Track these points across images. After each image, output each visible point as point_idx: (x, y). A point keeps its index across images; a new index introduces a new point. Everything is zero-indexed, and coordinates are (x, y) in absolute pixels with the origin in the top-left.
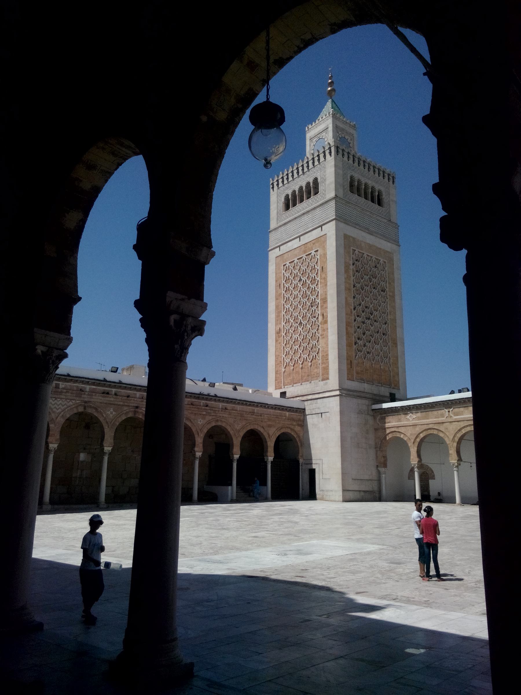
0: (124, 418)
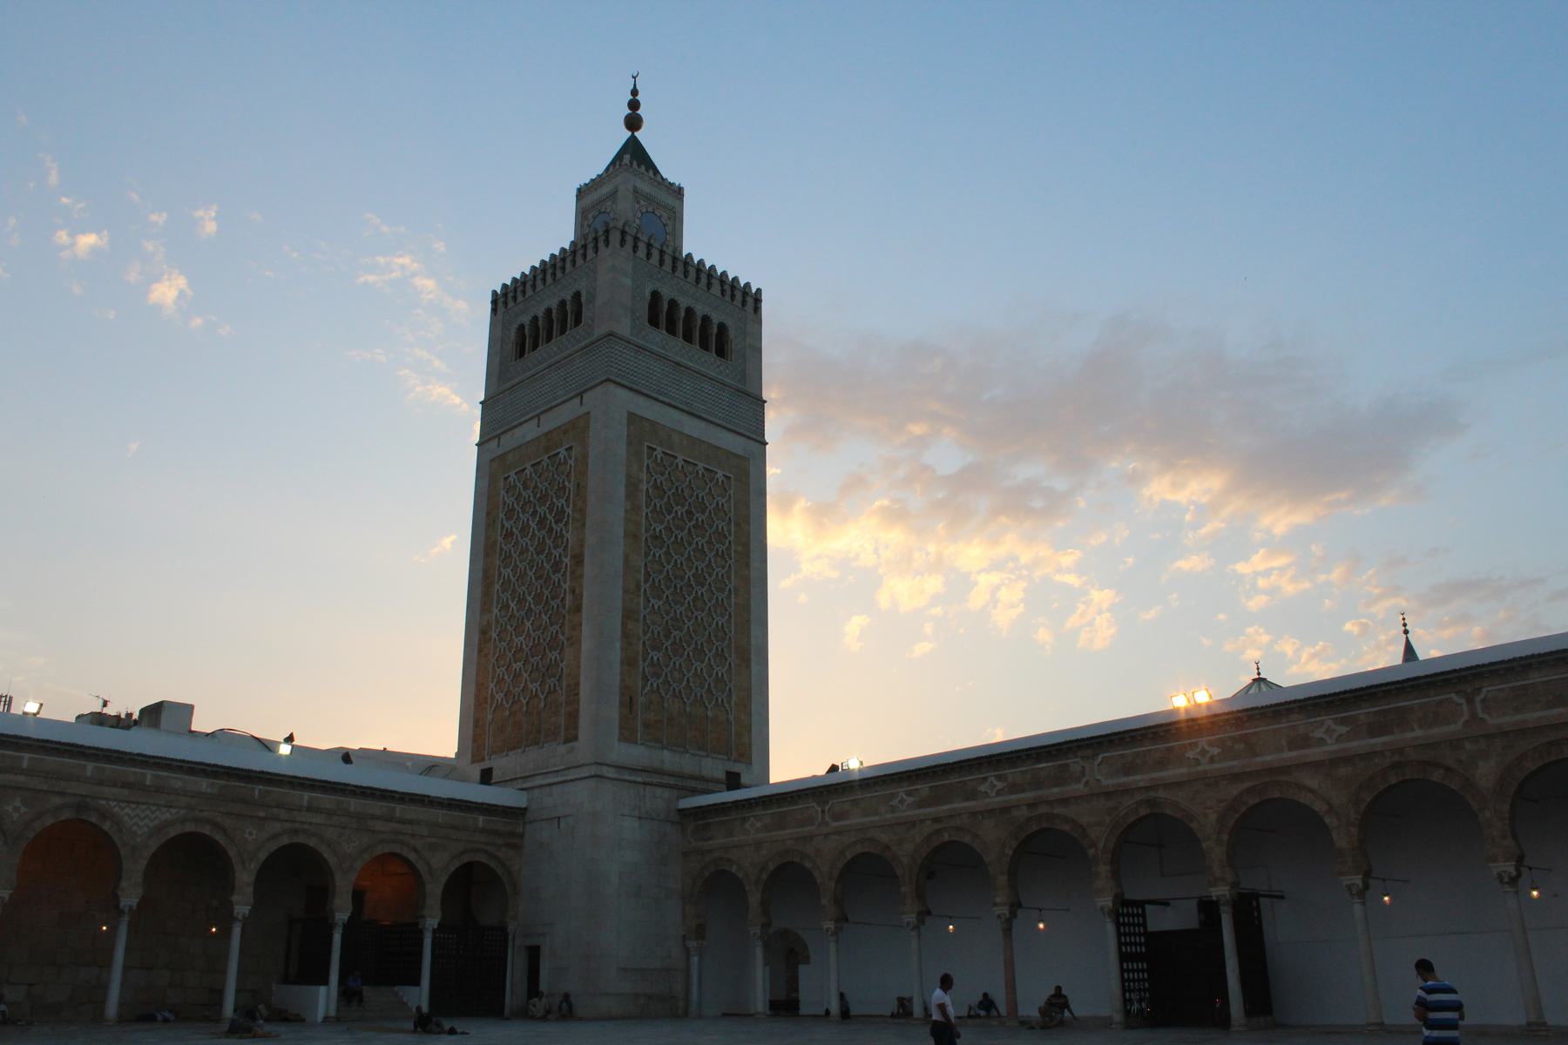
0: (49, 821)
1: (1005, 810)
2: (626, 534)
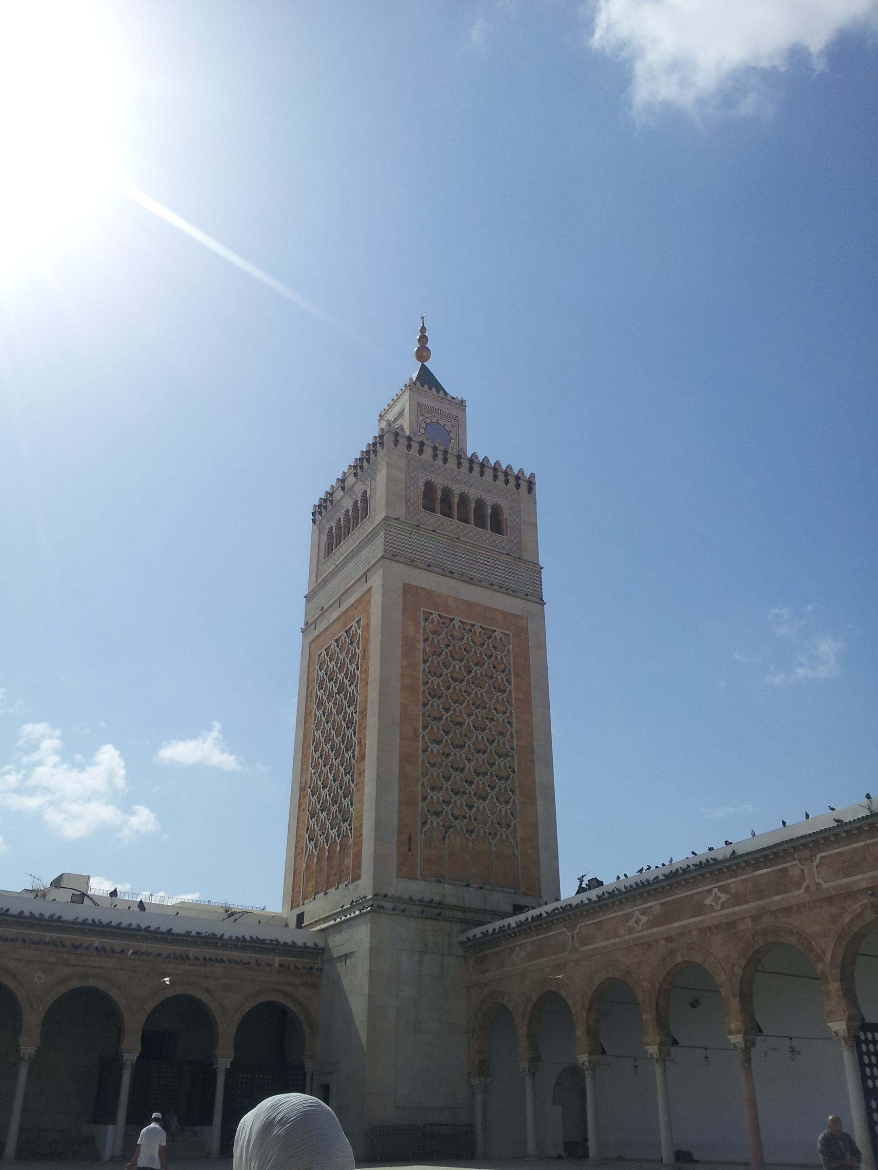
1: (731, 925)
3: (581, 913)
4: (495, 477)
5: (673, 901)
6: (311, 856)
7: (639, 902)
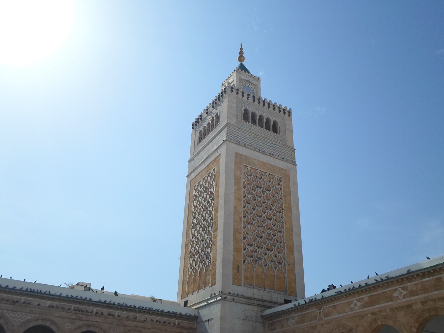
1: (409, 306)
2: (235, 198)
3: (325, 301)
4: (274, 109)
5: (376, 295)
6: (191, 275)
7: (356, 296)
